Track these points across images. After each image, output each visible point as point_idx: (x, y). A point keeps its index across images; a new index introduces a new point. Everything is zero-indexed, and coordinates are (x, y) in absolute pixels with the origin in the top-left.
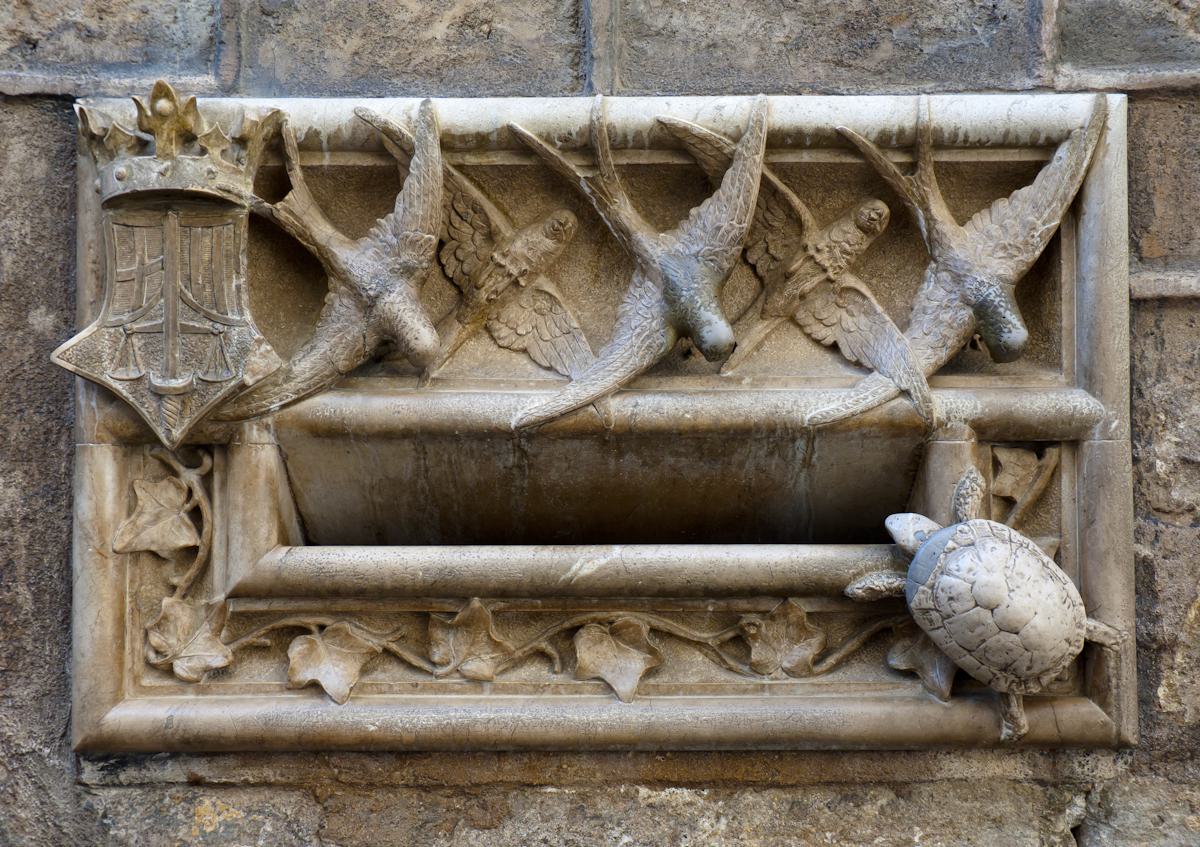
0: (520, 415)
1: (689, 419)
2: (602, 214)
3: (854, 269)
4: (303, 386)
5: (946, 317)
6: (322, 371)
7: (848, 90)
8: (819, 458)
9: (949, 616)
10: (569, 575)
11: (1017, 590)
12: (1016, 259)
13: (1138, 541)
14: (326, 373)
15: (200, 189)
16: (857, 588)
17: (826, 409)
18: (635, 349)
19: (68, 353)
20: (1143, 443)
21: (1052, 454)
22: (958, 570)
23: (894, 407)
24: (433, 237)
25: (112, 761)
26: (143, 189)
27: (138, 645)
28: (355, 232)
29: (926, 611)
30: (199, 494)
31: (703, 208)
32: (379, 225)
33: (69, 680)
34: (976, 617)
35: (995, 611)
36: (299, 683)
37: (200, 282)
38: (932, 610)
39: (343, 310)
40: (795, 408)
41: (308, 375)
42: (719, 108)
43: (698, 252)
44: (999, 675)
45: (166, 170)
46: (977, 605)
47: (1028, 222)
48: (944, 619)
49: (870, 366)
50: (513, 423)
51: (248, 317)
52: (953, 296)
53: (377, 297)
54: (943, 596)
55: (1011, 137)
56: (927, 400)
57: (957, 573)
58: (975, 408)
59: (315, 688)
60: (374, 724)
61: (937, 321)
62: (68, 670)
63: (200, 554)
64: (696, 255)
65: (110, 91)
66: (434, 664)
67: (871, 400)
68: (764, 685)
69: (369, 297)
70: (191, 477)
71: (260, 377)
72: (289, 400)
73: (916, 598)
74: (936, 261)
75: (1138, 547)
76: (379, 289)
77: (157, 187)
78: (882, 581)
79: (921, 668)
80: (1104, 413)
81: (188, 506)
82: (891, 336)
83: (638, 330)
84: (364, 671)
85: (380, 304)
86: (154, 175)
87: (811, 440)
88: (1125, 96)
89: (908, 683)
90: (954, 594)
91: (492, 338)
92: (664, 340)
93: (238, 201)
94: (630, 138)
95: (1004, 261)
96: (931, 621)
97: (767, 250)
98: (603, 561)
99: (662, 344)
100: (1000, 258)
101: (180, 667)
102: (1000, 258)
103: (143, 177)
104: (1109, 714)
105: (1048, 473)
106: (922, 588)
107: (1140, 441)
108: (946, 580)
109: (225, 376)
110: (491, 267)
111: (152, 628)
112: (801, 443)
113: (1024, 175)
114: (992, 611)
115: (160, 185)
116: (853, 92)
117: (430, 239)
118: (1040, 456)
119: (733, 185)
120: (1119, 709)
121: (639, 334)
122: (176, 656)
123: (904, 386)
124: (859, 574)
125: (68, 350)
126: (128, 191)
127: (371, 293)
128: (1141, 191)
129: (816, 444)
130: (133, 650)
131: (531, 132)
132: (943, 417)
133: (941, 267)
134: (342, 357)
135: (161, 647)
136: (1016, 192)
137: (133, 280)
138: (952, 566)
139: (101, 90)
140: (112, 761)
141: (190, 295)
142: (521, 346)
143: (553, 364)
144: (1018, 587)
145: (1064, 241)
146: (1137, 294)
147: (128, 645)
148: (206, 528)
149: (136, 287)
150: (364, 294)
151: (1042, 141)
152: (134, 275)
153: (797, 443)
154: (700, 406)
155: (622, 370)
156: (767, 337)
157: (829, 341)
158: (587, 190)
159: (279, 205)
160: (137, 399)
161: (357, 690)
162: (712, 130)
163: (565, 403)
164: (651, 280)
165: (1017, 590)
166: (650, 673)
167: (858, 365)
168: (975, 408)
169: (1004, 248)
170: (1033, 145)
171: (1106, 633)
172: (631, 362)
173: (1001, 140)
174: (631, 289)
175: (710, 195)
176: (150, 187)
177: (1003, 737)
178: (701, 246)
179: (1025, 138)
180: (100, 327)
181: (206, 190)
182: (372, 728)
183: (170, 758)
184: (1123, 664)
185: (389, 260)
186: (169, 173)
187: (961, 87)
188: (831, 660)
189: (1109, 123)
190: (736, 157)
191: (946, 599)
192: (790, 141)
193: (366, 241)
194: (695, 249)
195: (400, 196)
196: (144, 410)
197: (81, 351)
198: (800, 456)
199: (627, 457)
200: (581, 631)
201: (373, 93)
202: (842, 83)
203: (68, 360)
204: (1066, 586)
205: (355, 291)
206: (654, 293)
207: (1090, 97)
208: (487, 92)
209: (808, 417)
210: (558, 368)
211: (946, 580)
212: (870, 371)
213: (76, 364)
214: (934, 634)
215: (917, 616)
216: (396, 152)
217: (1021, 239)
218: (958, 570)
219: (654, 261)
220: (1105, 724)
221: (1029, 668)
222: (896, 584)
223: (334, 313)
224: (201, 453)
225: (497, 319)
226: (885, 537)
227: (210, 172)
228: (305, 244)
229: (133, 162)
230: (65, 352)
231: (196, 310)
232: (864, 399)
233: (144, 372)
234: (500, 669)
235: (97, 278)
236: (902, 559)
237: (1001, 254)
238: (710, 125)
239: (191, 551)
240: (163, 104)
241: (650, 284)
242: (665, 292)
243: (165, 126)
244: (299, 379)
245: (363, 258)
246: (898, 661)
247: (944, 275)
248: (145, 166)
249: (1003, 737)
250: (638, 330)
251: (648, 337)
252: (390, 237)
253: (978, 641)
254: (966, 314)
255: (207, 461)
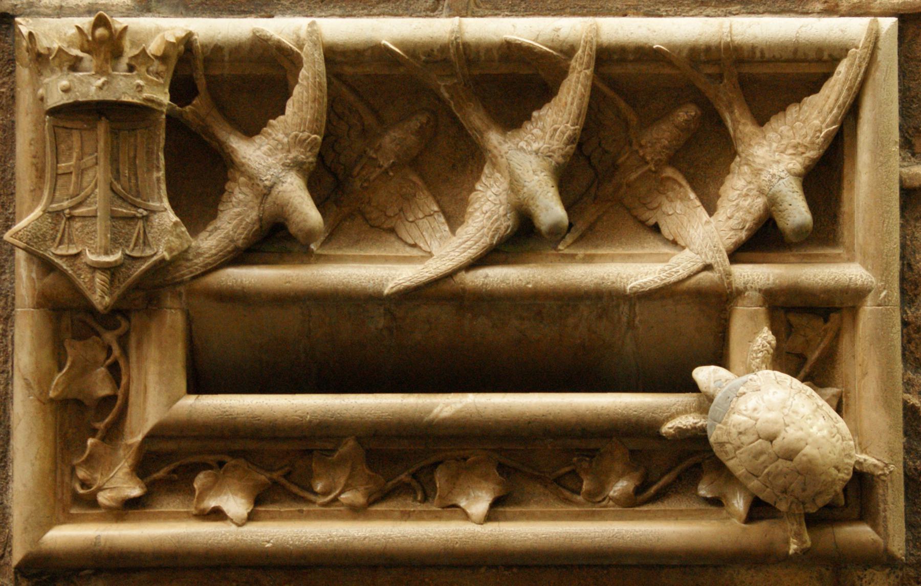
0: (391, 285)
1: (530, 289)
2: (458, 115)
3: (672, 161)
4: (209, 261)
5: (746, 203)
6: (226, 248)
7: (667, 11)
8: (640, 321)
9: (739, 448)
10: (432, 416)
11: (792, 425)
12: (804, 155)
13: (907, 391)
14: (229, 249)
15: (130, 100)
16: (668, 428)
17: (645, 280)
18: (486, 230)
19: (20, 233)
20: (913, 309)
21: (834, 317)
22: (745, 410)
23: (700, 279)
24: (318, 137)
25: (44, 578)
26: (84, 99)
27: (67, 479)
28: (251, 130)
29: (722, 444)
30: (116, 352)
31: (543, 112)
32: (272, 126)
33: (7, 510)
34: (759, 447)
35: (774, 442)
36: (204, 510)
37: (127, 175)
38: (727, 443)
39: (241, 196)
40: (619, 279)
41: (214, 252)
42: (558, 30)
43: (539, 149)
44: (781, 497)
45: (104, 84)
46: (760, 438)
47: (814, 125)
48: (736, 450)
49: (683, 244)
50: (386, 291)
51: (166, 204)
52: (752, 186)
53: (272, 187)
54: (734, 431)
55: (800, 55)
56: (729, 274)
57: (745, 413)
58: (768, 279)
59: (217, 515)
60: (268, 542)
61: (738, 207)
62: (5, 502)
63: (119, 402)
64: (537, 152)
65: (42, 10)
66: (316, 494)
67: (682, 273)
68: (594, 511)
69: (265, 187)
70: (110, 337)
71: (175, 253)
72: (199, 272)
73: (714, 434)
74: (740, 157)
75: (907, 396)
76: (273, 180)
77: (96, 98)
78: (687, 421)
79: (725, 496)
80: (875, 283)
81: (109, 361)
82: (700, 218)
83: (488, 215)
84: (258, 501)
85: (274, 192)
86: (93, 89)
87: (632, 307)
88: (894, 20)
89: (714, 508)
90: (742, 429)
91: (366, 220)
92: (507, 224)
93: (159, 109)
94: (482, 54)
95: (794, 157)
96: (726, 453)
97: (600, 143)
98: (459, 406)
99: (508, 226)
100: (791, 154)
101: (103, 498)
102: (791, 154)
103: (84, 90)
104: (878, 533)
105: (830, 335)
106: (719, 425)
107: (910, 308)
108: (736, 418)
109: (148, 252)
110: (364, 160)
111: (79, 465)
112: (625, 308)
113: (814, 85)
114: (771, 442)
115: (98, 96)
116: (670, 13)
117: (316, 139)
118: (826, 320)
119: (568, 93)
120: (886, 528)
121: (489, 218)
122: (100, 489)
123: (709, 261)
124: (672, 417)
125: (20, 231)
126: (71, 101)
127: (267, 183)
128: (913, 97)
129: (637, 308)
130: (63, 482)
131: (400, 49)
132: (741, 287)
133: (743, 162)
134: (243, 236)
135: (87, 480)
136: (805, 99)
137: (71, 173)
138: (742, 407)
139: (34, 9)
140: (44, 578)
141: (119, 187)
142: (389, 226)
143: (417, 241)
144: (793, 423)
145: (847, 139)
146: (908, 183)
147: (59, 479)
148: (124, 381)
149: (73, 178)
150: (261, 184)
151: (826, 57)
152: (72, 169)
153: (621, 309)
154: (539, 277)
155: (475, 247)
156: (599, 218)
157: (652, 222)
158: (446, 95)
159: (188, 108)
160: (75, 272)
161: (252, 517)
162: (550, 48)
163: (428, 275)
164: (499, 172)
165: (792, 425)
166: (496, 503)
167: (674, 243)
168: (768, 279)
169: (795, 147)
170: (819, 60)
171: (875, 466)
172: (482, 241)
173: (791, 56)
174: (483, 178)
175: (549, 101)
176: (89, 98)
177: (791, 552)
178: (541, 143)
179: (812, 55)
180: (44, 211)
181: (135, 101)
182: (268, 545)
183: (94, 574)
184: (890, 491)
185: (280, 156)
186: (105, 88)
187: (761, 9)
188: (652, 490)
189: (881, 44)
190: (570, 70)
191: (737, 433)
192: (616, 57)
193: (258, 139)
194: (535, 146)
195: (290, 103)
196: (81, 281)
197: (30, 232)
198: (624, 319)
199: (479, 320)
200: (440, 466)
201: (266, 12)
202: (661, 5)
203: (20, 239)
204: (837, 425)
205: (252, 179)
206: (501, 183)
207: (865, 21)
208: (361, 12)
209: (628, 288)
210: (422, 245)
211: (736, 418)
212: (683, 248)
213: (26, 243)
214: (730, 464)
215: (716, 448)
216: (287, 65)
217: (808, 138)
218: (745, 410)
219: (502, 157)
220: (875, 541)
221: (804, 490)
222: (700, 424)
223: (234, 199)
224: (119, 318)
225: (369, 203)
226: (692, 387)
227: (139, 86)
228: (208, 140)
229: (75, 77)
230: (17, 233)
231: (124, 199)
232: (676, 272)
233: (80, 249)
234: (372, 498)
235: (37, 170)
236: (706, 403)
237: (791, 151)
238: (549, 44)
239: (110, 400)
240: (100, 32)
241: (498, 175)
242: (511, 183)
243: (103, 49)
244: (207, 255)
245: (258, 153)
246: (704, 491)
247: (745, 169)
248: (85, 80)
249: (791, 552)
250: (488, 215)
251: (497, 220)
252: (281, 136)
253: (762, 468)
254: (760, 202)
255: (124, 324)
